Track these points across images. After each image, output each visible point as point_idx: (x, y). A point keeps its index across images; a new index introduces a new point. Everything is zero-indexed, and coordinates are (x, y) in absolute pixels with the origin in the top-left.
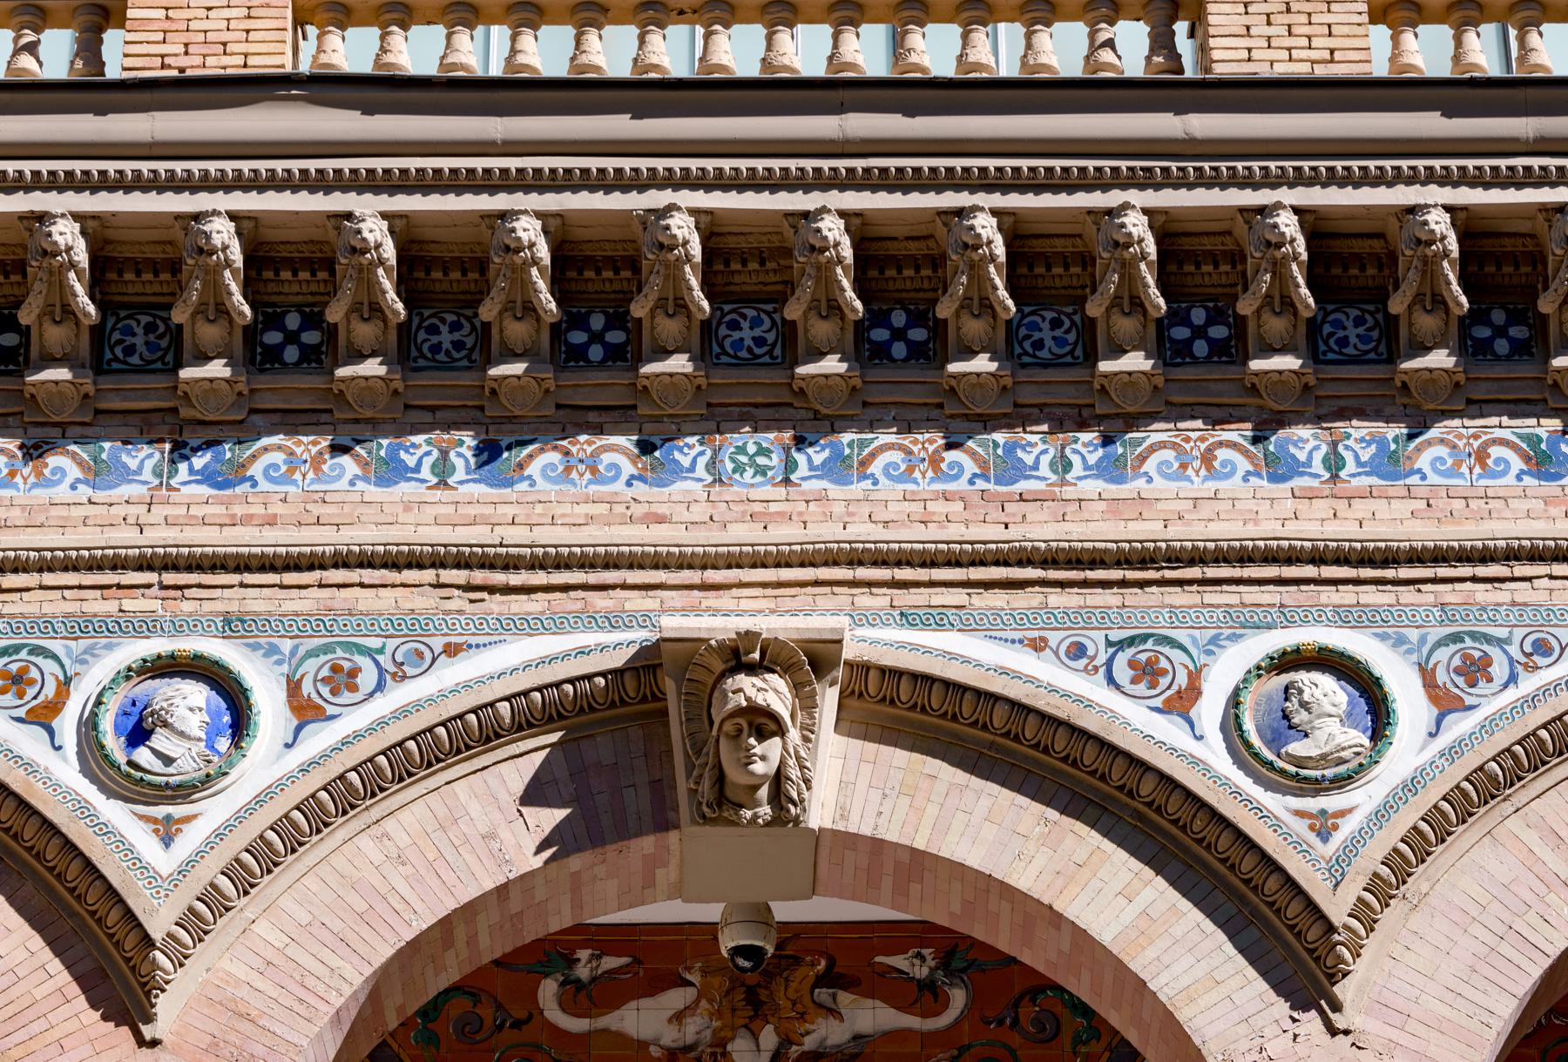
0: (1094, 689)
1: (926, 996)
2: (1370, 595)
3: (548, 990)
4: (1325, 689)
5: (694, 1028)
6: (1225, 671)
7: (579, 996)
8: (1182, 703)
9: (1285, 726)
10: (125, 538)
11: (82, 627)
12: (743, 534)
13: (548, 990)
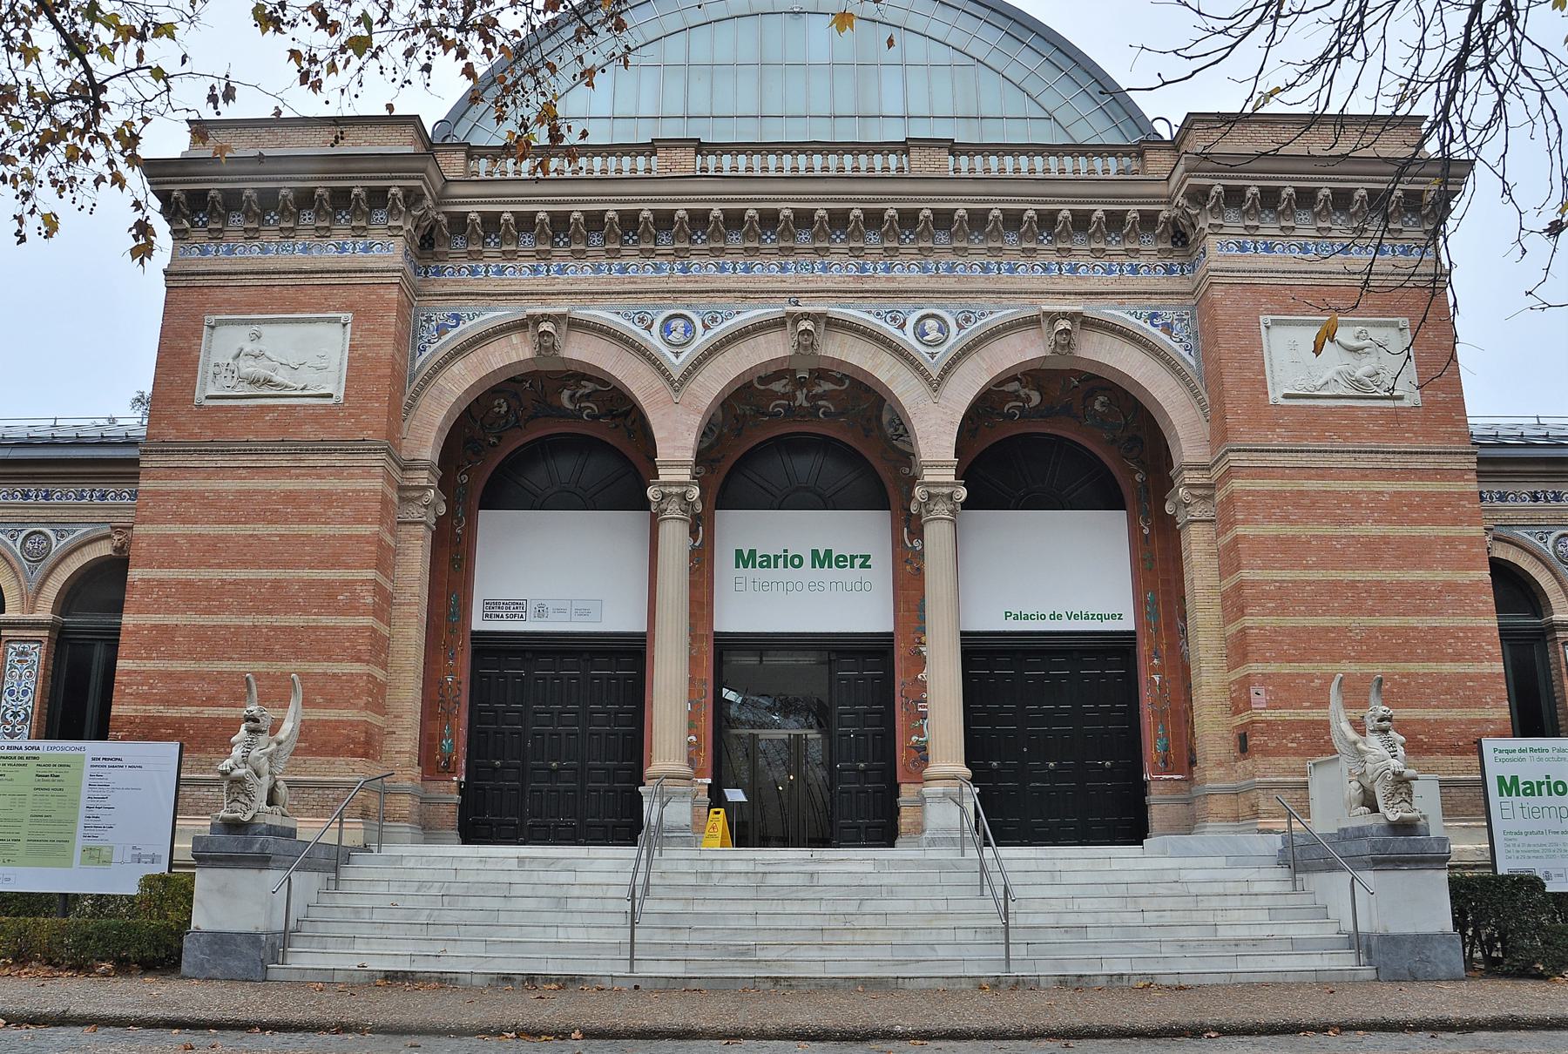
1: (840, 381)
2: (945, 302)
4: (931, 323)
6: (912, 320)
8: (902, 327)
11: (657, 306)
12: (803, 286)
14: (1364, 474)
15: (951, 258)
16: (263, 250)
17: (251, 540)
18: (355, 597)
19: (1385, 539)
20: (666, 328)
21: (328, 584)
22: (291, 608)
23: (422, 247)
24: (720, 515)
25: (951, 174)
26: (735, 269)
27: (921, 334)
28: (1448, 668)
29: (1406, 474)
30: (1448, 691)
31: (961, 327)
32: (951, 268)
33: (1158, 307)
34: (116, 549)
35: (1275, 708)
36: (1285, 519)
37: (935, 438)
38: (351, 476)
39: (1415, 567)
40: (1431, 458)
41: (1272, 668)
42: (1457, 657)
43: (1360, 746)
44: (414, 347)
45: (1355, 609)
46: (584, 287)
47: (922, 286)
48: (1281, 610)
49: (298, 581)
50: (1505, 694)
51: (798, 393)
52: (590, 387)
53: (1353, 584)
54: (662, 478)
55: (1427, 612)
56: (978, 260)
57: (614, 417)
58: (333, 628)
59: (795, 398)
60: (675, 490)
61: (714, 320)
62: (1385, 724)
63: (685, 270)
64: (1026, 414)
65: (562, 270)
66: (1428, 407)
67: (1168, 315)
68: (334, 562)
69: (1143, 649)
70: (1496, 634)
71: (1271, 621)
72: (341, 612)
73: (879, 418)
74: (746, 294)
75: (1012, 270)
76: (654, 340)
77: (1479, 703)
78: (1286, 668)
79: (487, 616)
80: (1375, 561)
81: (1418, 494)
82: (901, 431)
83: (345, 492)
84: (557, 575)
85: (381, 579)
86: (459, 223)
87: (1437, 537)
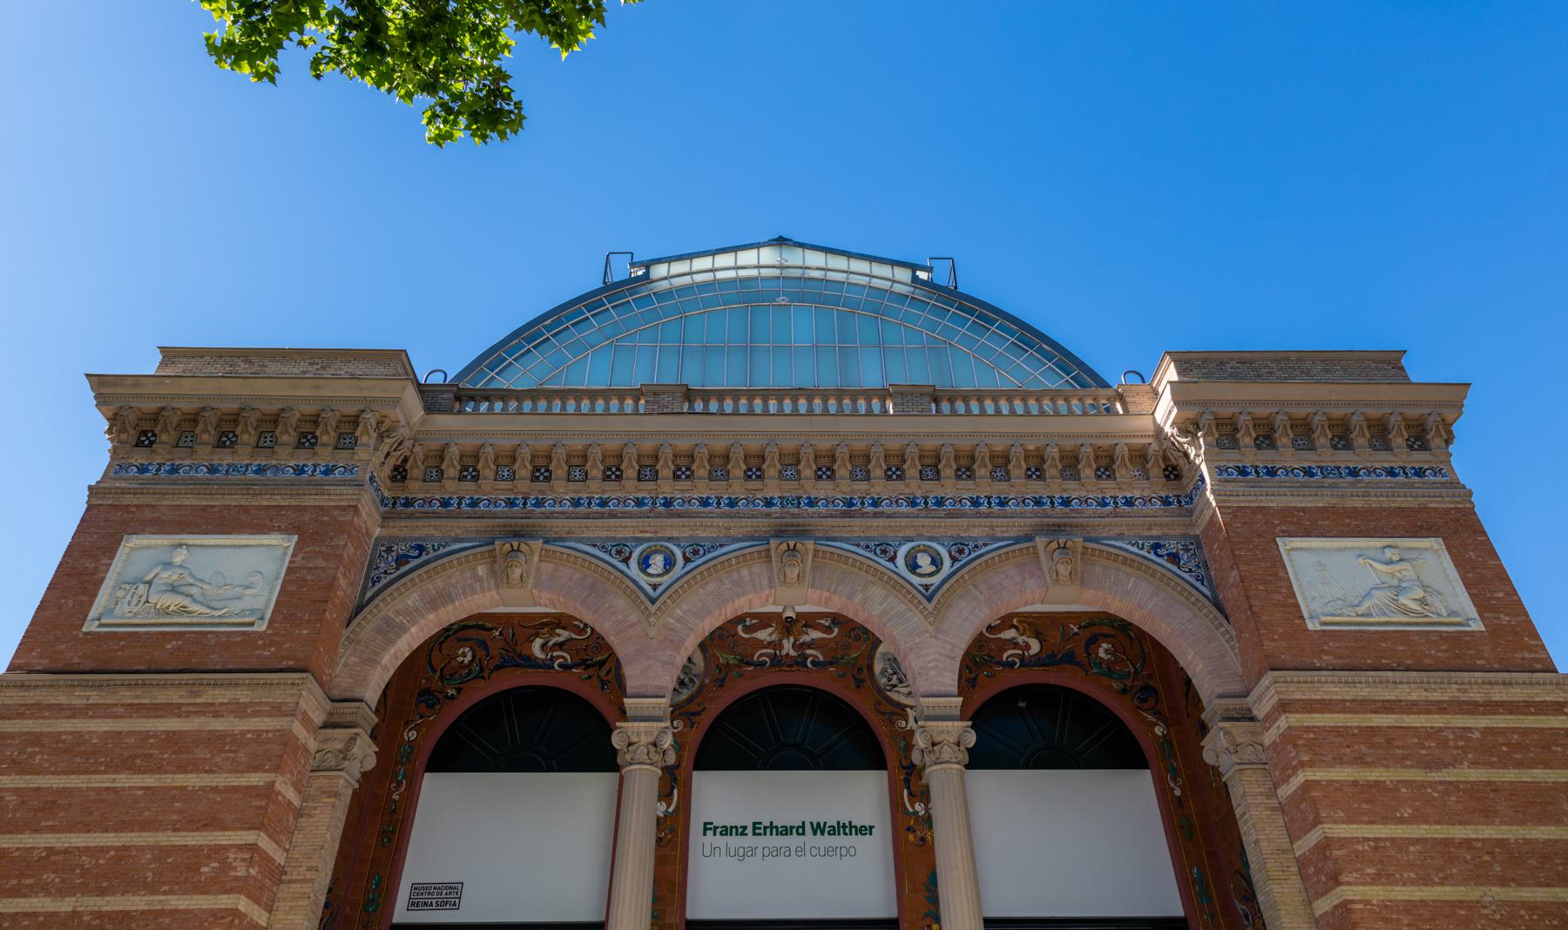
1: (828, 630)
3: (740, 628)
5: (774, 637)
6: (902, 551)
7: (747, 629)
8: (892, 559)
13: (740, 628)
14: (1440, 708)
17: (104, 796)
18: (225, 866)
21: (195, 851)
22: (131, 885)
23: (393, 479)
24: (698, 776)
26: (719, 503)
29: (1491, 707)
31: (954, 559)
33: (1159, 537)
38: (256, 714)
44: (367, 578)
45: (1479, 875)
49: (152, 848)
51: (785, 642)
52: (564, 635)
53: (1467, 843)
57: (587, 667)
58: (184, 912)
59: (781, 647)
64: (1026, 662)
66: (1494, 631)
67: (1172, 546)
68: (212, 822)
71: (1376, 893)
72: (202, 889)
73: (870, 667)
80: (1488, 816)
81: (1515, 730)
82: (895, 680)
83: (243, 733)
85: (264, 841)
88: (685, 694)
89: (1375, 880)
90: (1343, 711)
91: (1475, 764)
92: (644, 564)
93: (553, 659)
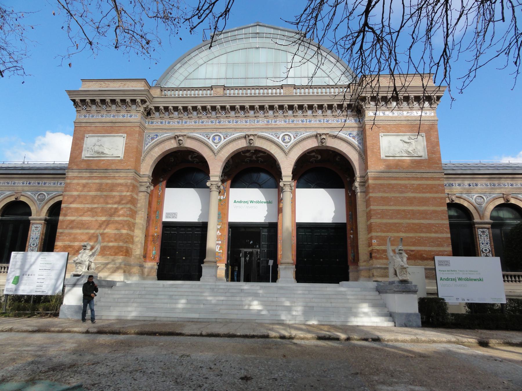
0: (273, 137)
4: (287, 137)
8: (278, 138)
9: (284, 140)
10: (214, 127)
12: (251, 127)
14: (409, 179)
15: (293, 118)
16: (102, 116)
19: (415, 198)
20: (214, 139)
23: (147, 115)
25: (294, 94)
27: (283, 140)
28: (433, 235)
29: (422, 178)
30: (432, 242)
32: (293, 121)
34: (16, 199)
35: (379, 246)
36: (384, 192)
37: (287, 168)
39: (423, 205)
40: (430, 174)
41: (379, 234)
42: (436, 232)
43: (394, 257)
46: (192, 127)
47: (285, 126)
48: (382, 217)
50: (450, 243)
54: (211, 180)
55: (427, 219)
56: (300, 119)
60: (214, 183)
61: (227, 136)
62: (401, 251)
63: (219, 122)
65: (186, 123)
69: (348, 227)
70: (448, 225)
71: (378, 221)
74: (235, 129)
75: (310, 121)
76: (210, 142)
77: (442, 246)
78: (383, 234)
79: (167, 217)
84: (182, 205)
86: (157, 109)
87: (431, 197)
88: (227, 170)
89: (379, 218)
90: (384, 180)
91: (412, 192)
92: (214, 139)
93: (194, 161)
